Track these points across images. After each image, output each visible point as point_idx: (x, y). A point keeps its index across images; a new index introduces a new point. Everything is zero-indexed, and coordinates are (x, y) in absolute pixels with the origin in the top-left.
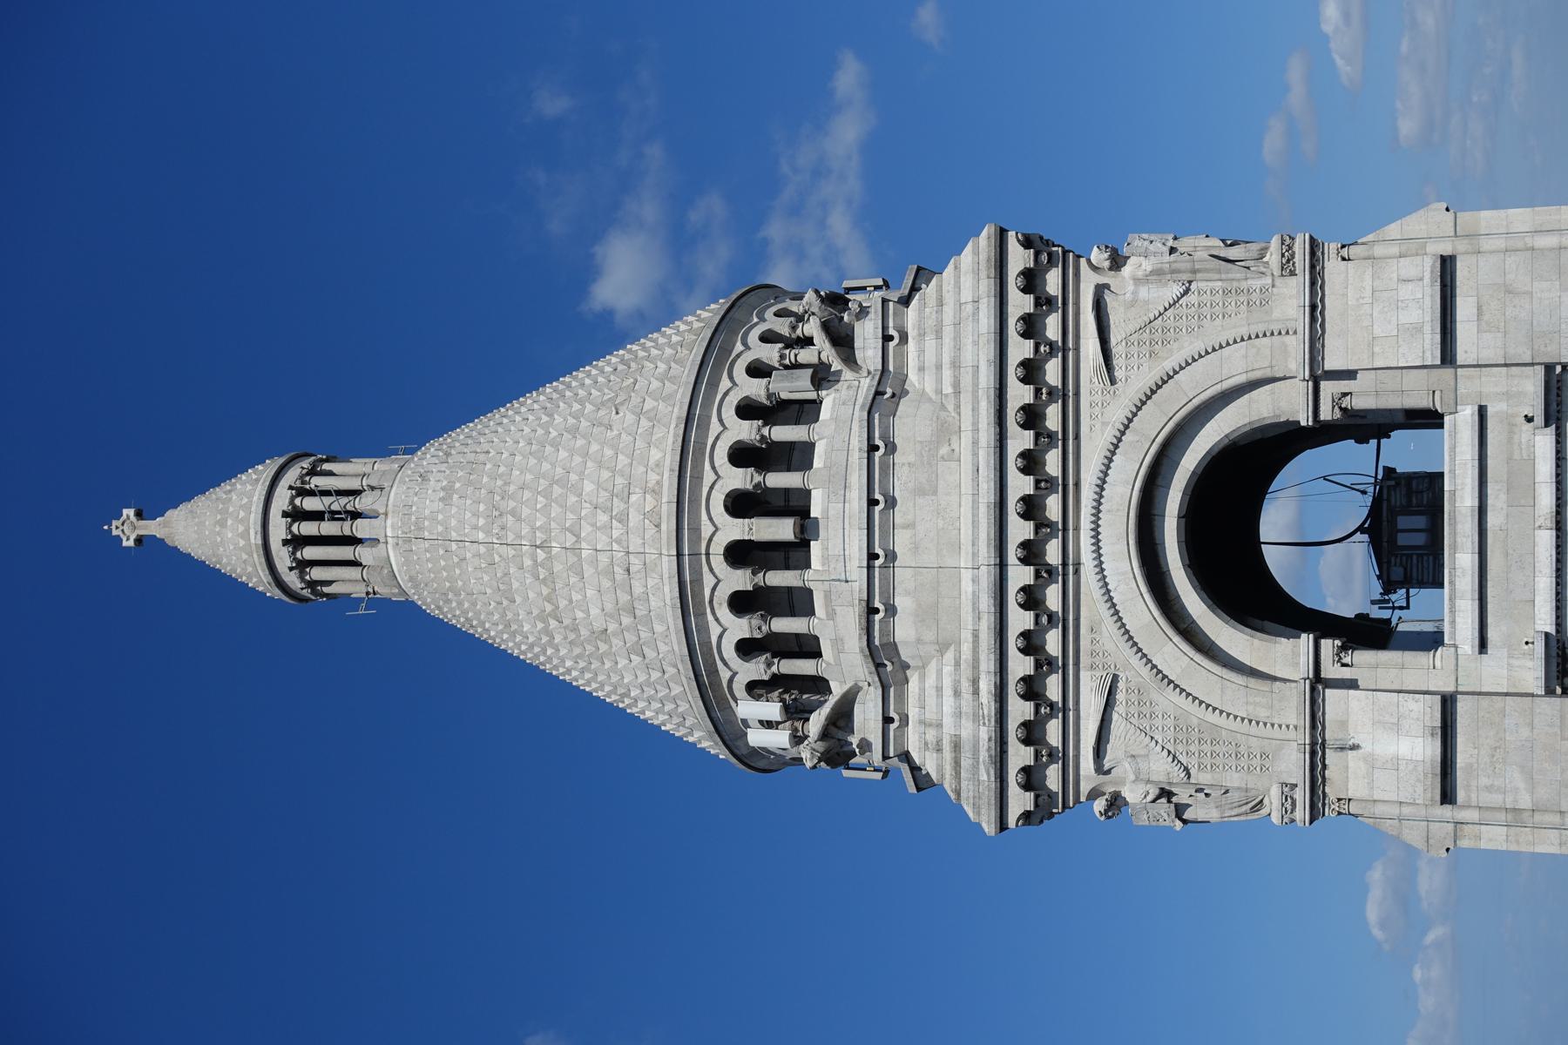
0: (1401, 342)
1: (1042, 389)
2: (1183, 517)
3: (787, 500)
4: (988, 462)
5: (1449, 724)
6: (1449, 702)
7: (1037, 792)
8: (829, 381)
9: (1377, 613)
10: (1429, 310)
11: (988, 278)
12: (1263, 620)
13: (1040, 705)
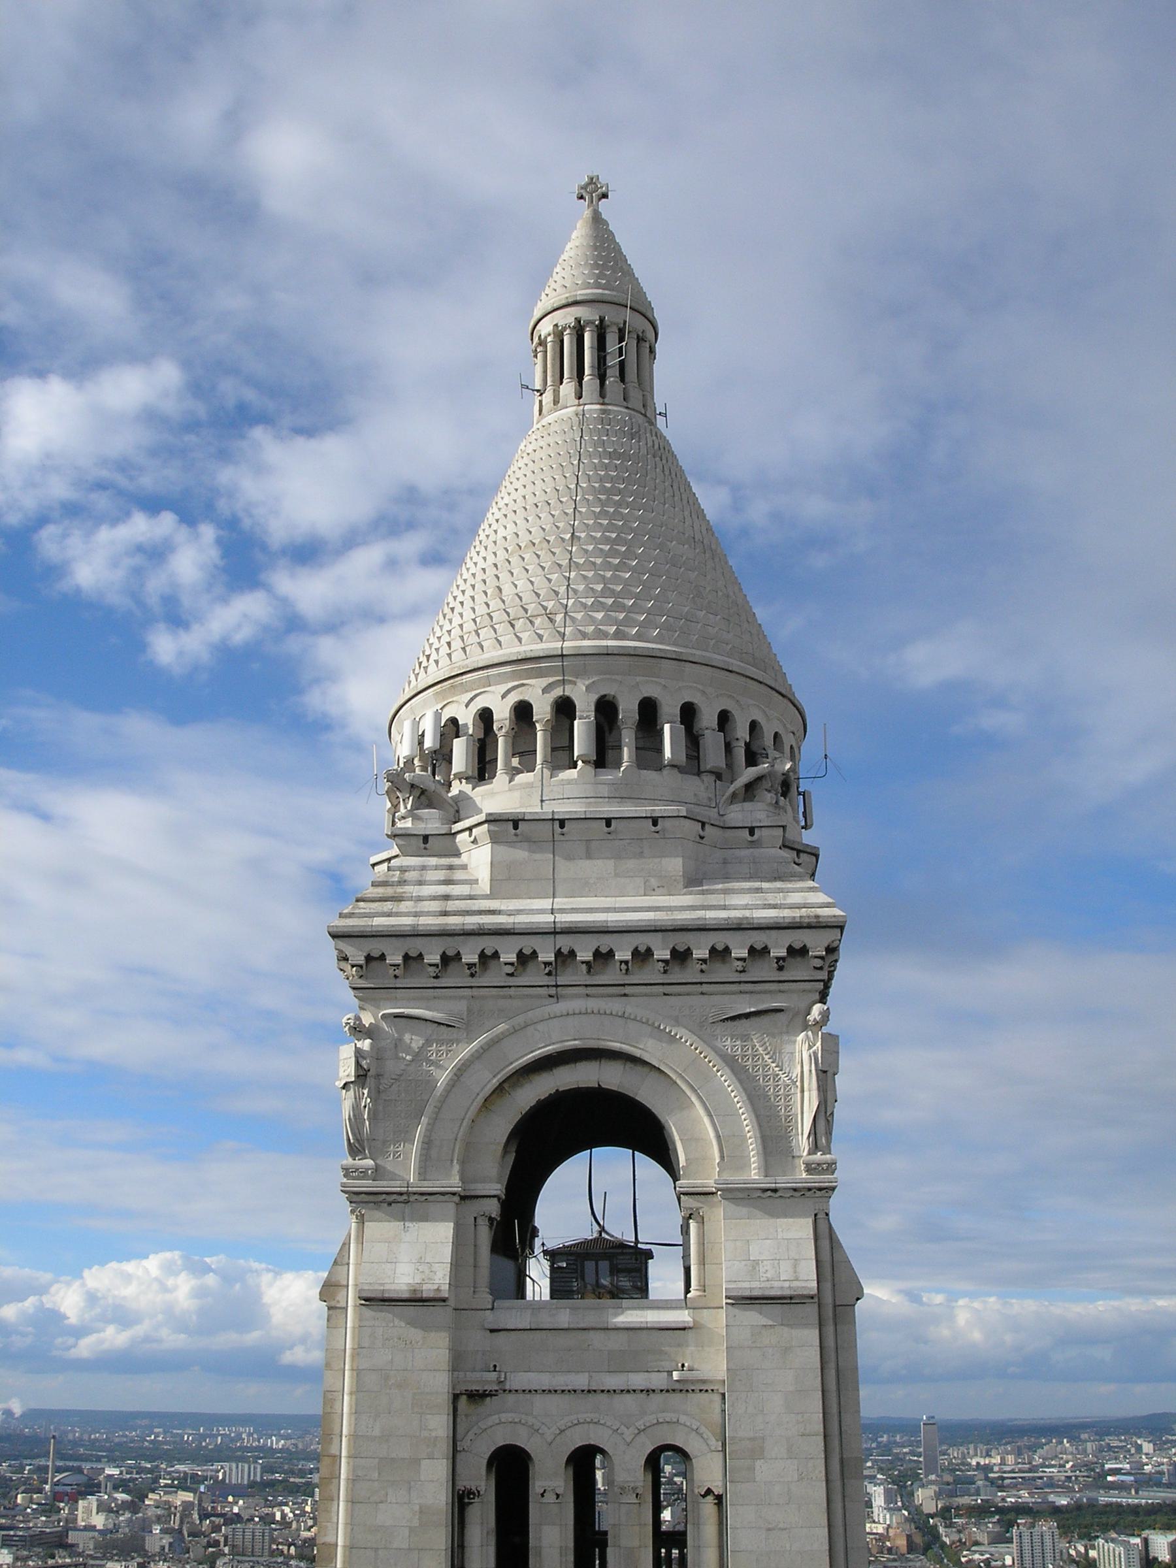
0: (744, 1263)
1: (706, 964)
2: (599, 1085)
3: (613, 748)
4: (642, 920)
5: (425, 1304)
6: (444, 1304)
7: (364, 967)
8: (715, 781)
9: (538, 1242)
10: (769, 1286)
11: (801, 917)
12: (516, 1152)
13: (438, 967)
